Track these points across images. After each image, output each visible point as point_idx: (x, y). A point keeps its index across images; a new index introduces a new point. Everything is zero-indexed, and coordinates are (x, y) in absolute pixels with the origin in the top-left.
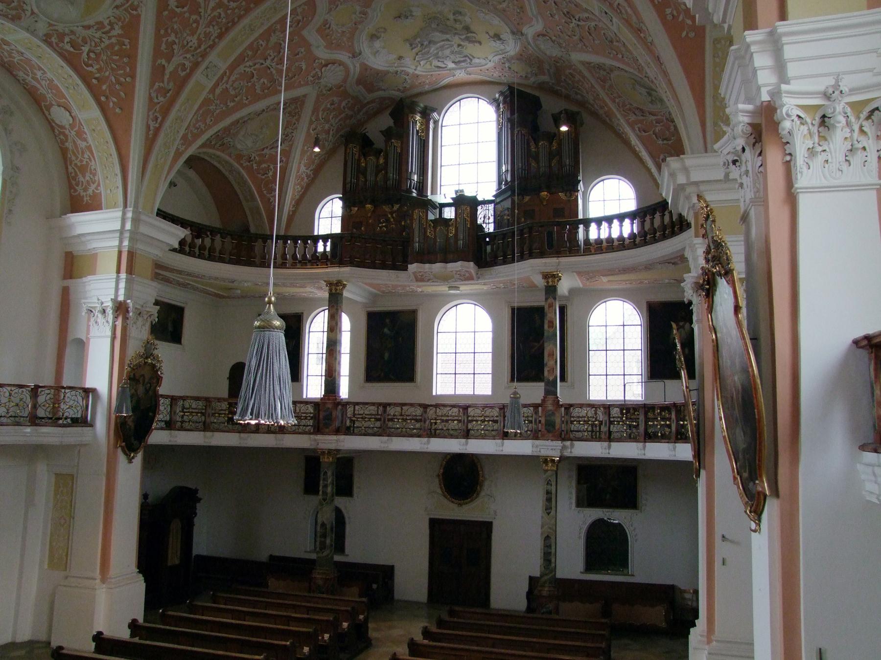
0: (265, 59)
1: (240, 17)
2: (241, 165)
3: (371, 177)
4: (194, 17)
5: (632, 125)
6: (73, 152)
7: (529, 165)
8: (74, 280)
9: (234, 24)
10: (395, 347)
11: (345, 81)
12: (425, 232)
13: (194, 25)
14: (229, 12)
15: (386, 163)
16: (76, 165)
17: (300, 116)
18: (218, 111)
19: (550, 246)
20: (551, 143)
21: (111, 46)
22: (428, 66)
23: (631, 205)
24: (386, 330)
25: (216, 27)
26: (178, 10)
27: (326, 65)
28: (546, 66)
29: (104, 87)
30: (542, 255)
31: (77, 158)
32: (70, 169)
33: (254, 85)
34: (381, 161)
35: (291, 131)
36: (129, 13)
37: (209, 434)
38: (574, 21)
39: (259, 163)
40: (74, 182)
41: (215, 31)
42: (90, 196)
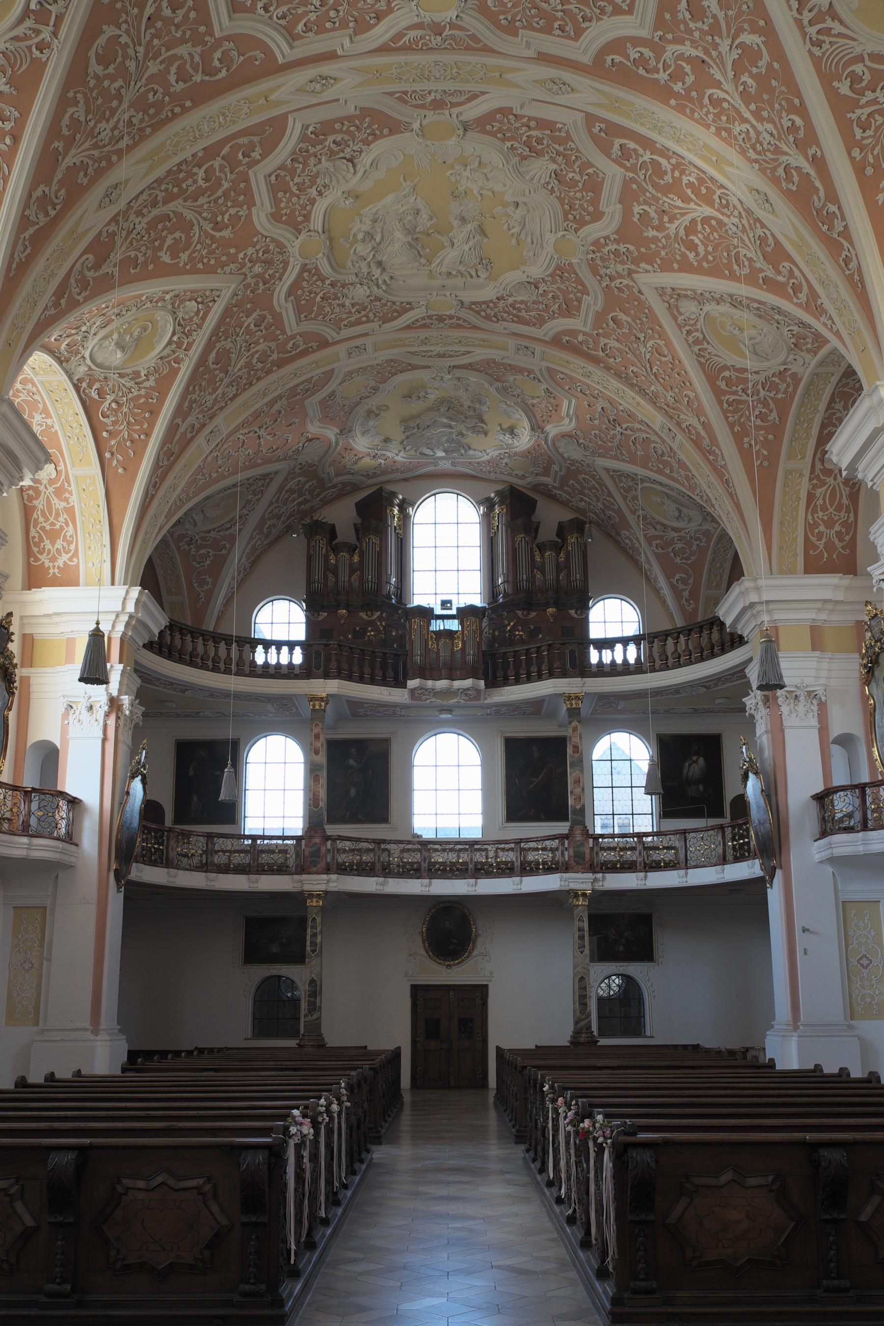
3: (343, 576)
4: (222, 375)
5: (649, 540)
6: (43, 512)
7: (533, 576)
8: (32, 670)
10: (358, 779)
12: (427, 644)
14: (252, 372)
15: (361, 561)
16: (43, 528)
19: (573, 666)
20: (558, 554)
21: (139, 397)
22: (412, 452)
23: (632, 628)
24: (351, 762)
28: (556, 468)
29: (113, 442)
30: (564, 675)
31: (47, 520)
32: (33, 532)
35: (247, 512)
36: (170, 365)
37: (173, 871)
38: (619, 429)
40: (35, 549)
42: (59, 568)
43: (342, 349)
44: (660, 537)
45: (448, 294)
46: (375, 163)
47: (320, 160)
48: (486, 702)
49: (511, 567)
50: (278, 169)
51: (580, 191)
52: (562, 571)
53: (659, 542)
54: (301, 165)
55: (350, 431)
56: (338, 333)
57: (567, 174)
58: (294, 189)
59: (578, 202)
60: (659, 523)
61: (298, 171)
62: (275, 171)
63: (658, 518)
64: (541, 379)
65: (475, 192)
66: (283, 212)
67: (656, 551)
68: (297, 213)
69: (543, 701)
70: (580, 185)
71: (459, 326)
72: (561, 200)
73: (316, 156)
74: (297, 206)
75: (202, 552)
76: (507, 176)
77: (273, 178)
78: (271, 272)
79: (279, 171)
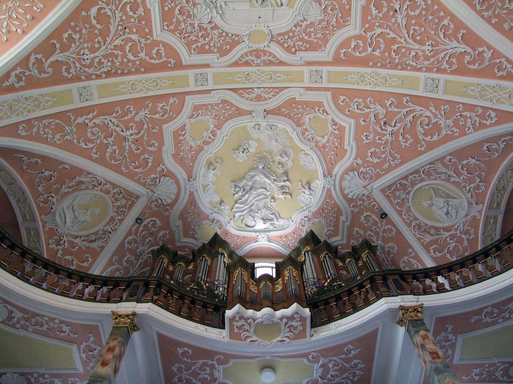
0: (128, 129)
1: (130, 73)
2: (48, 244)
5: (426, 247)
9: (123, 74)
11: (172, 205)
13: (97, 46)
14: (125, 60)
17: (125, 216)
18: (69, 137)
25: (109, 64)
26: (94, 22)
27: (166, 176)
33: (107, 146)
34: (191, 267)
39: (66, 252)
41: (107, 66)
43: (191, 73)
44: (435, 241)
45: (262, 25)
48: (313, 338)
49: (319, 271)
52: (362, 270)
53: (434, 246)
55: (195, 180)
56: (190, 57)
60: (432, 227)
63: (430, 223)
64: (329, 112)
67: (434, 256)
69: (375, 333)
71: (270, 63)
75: (67, 257)
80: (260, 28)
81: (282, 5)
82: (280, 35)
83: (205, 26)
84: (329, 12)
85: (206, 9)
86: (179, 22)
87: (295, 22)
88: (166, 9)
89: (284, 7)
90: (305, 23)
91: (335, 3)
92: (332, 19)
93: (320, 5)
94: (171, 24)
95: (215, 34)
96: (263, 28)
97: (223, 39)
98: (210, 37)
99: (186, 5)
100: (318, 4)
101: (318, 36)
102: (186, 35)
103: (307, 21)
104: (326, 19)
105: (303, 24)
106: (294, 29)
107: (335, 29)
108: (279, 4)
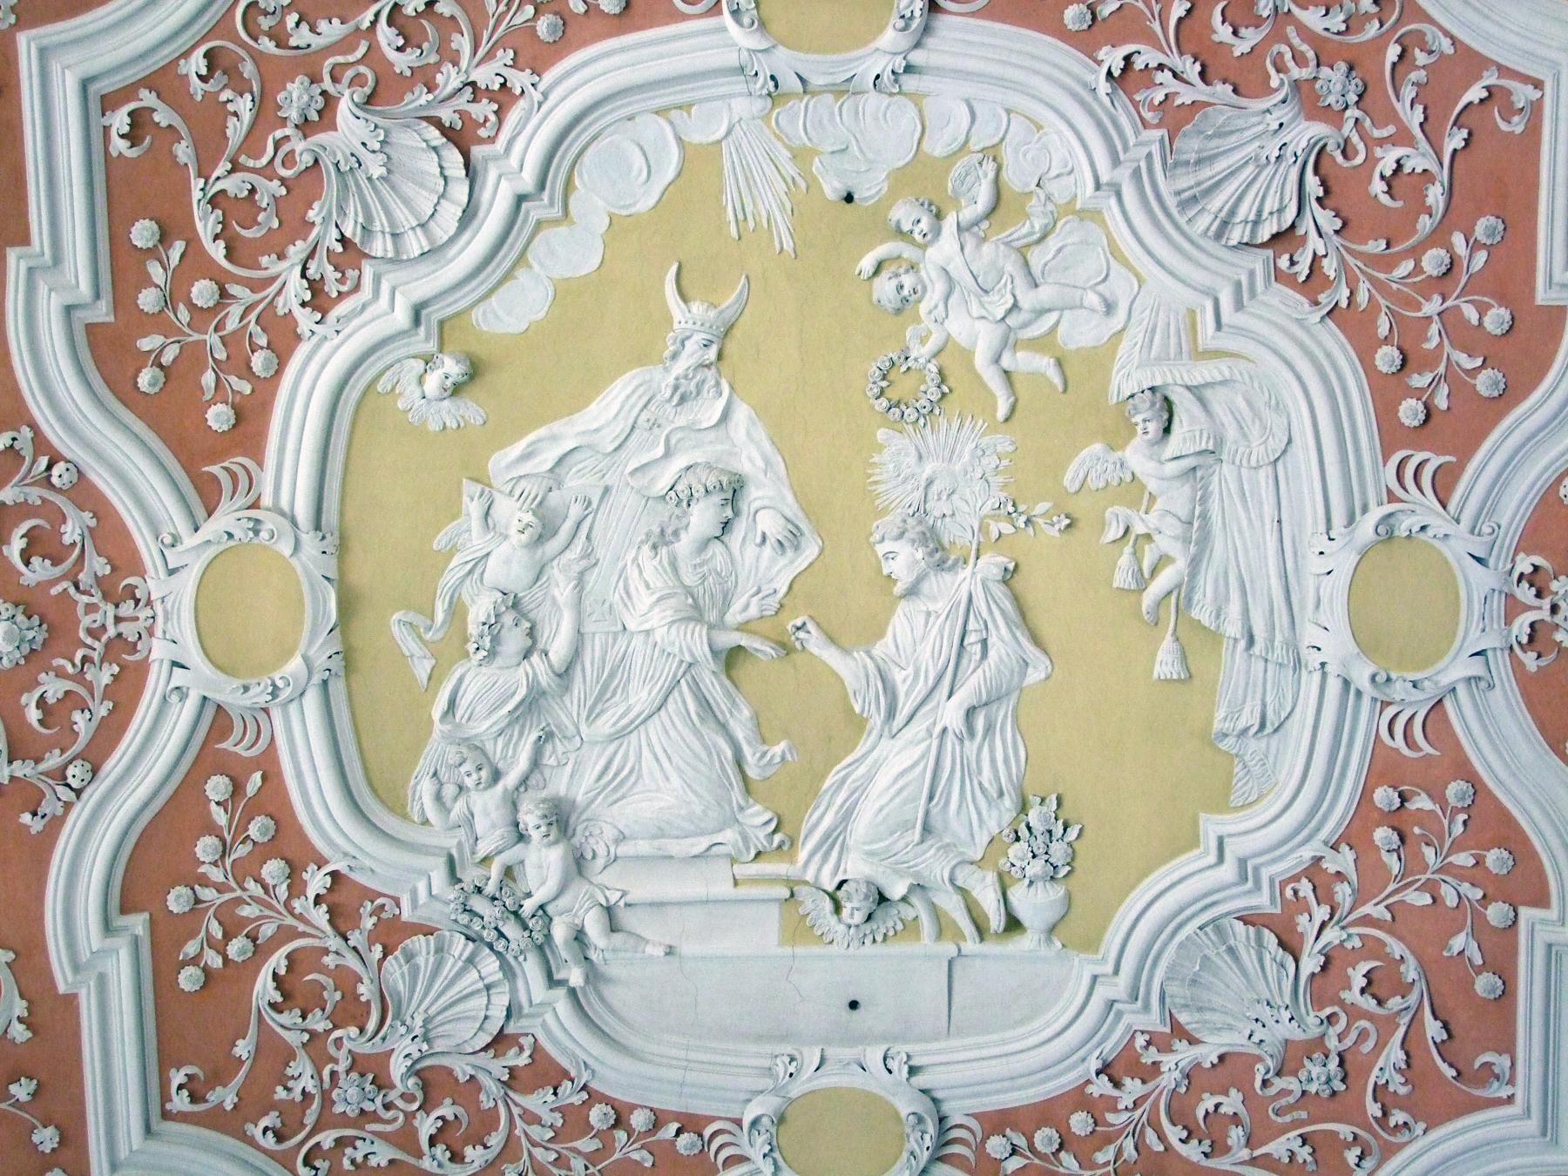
45: (874, 1056)
46: (557, 181)
47: (329, 100)
50: (148, 82)
51: (1438, 236)
54: (244, 105)
57: (1371, 161)
58: (206, 225)
59: (1432, 307)
61: (235, 131)
62: (129, 92)
65: (981, 360)
66: (147, 344)
68: (208, 379)
70: (1435, 195)
72: (1351, 322)
73: (315, 79)
74: (212, 339)
76: (1115, 252)
77: (120, 120)
78: (54, 688)
79: (147, 98)
80: (856, 1080)
81: (1013, 924)
82: (997, 1122)
83: (462, 1069)
84: (1353, 996)
85: (471, 961)
86: (274, 1055)
87: (1111, 1047)
88: (189, 979)
89: (1026, 943)
90: (1184, 1054)
91: (1396, 948)
92: (1380, 1046)
93: (1290, 946)
94: (219, 1077)
95: (531, 1118)
96: (876, 1081)
97: (587, 1145)
98: (496, 1140)
99: (334, 942)
100: (1270, 939)
101: (1277, 1148)
102: (327, 1139)
103: (1193, 1041)
104: (1332, 1043)
105: (1168, 1061)
106: (1102, 1086)
107: (1398, 1117)
108: (996, 921)
